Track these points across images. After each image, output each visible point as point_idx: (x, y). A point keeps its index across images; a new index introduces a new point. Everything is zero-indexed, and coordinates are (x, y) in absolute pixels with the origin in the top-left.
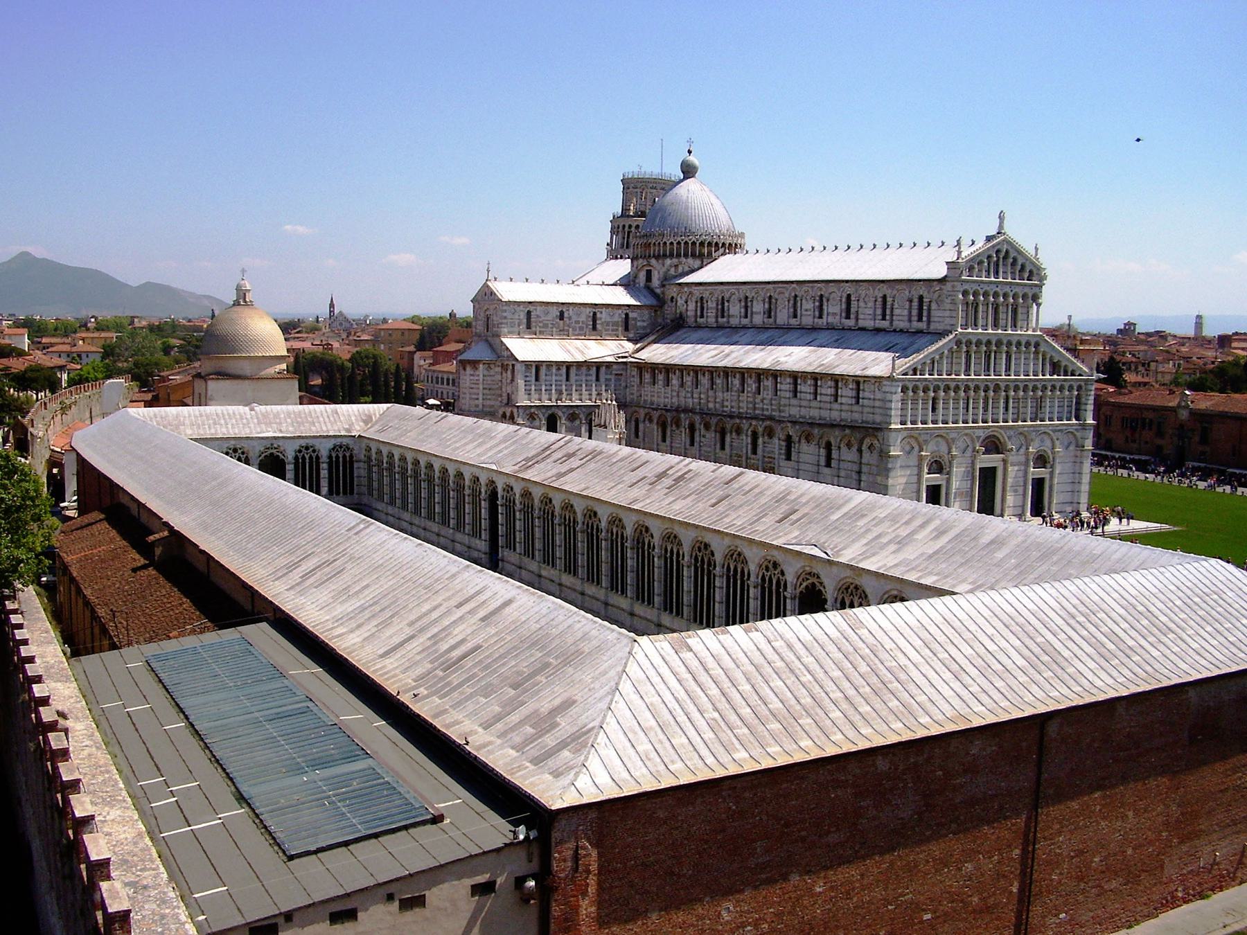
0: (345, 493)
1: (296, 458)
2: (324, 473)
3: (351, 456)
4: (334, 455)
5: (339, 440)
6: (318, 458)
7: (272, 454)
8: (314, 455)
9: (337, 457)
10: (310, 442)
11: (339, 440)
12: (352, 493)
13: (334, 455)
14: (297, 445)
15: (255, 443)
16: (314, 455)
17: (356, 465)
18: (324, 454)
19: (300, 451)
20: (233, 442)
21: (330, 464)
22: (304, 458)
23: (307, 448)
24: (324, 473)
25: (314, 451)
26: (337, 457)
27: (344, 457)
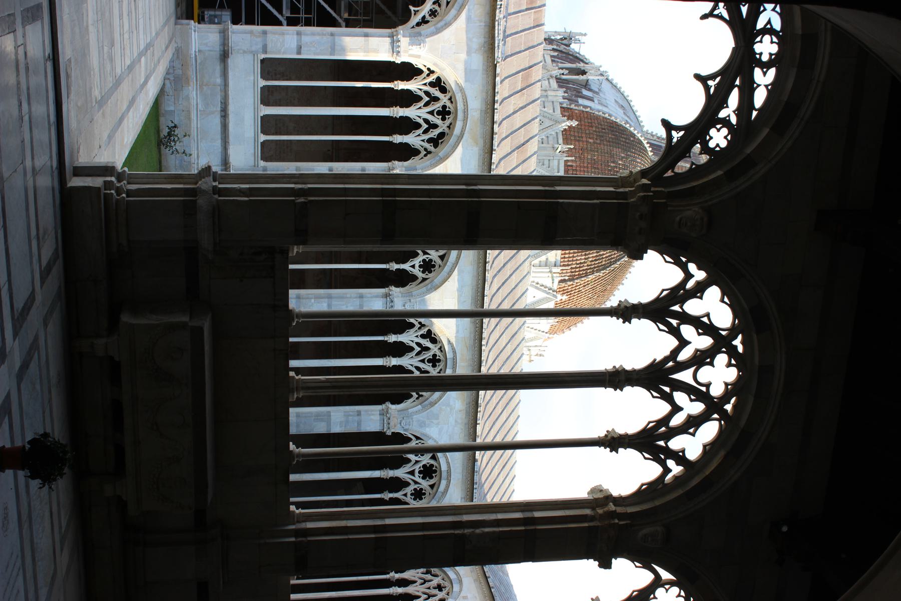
22: (398, 461)
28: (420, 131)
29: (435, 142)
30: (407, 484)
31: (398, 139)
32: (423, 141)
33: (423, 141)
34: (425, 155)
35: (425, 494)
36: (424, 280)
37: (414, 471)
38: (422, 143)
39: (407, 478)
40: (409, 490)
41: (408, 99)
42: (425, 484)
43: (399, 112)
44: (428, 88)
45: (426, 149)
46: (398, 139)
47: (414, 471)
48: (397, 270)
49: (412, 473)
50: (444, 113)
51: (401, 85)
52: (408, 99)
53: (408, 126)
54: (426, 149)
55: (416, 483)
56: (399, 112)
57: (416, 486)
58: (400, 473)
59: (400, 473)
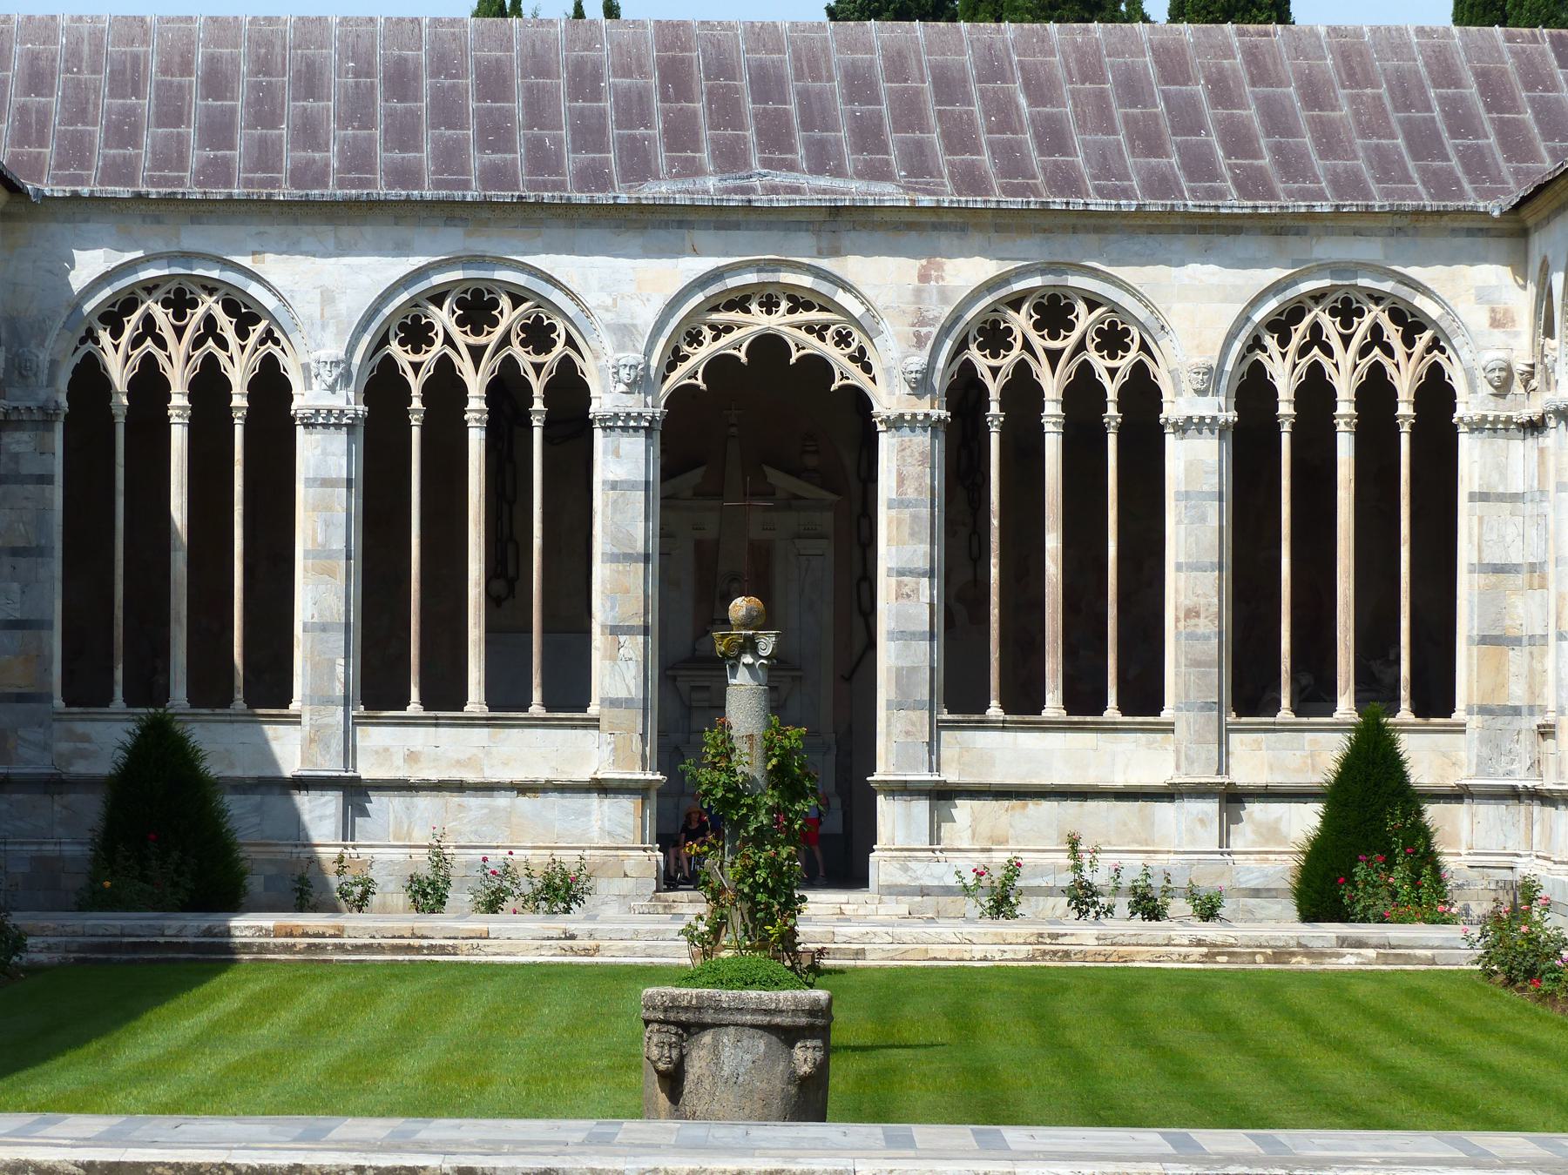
3: (1436, 393)
6: (1142, 393)
7: (769, 346)
13: (1284, 377)
21: (1250, 439)
22: (1023, 390)
28: (222, 356)
30: (1086, 369)
32: (243, 348)
33: (243, 348)
34: (277, 342)
35: (1113, 324)
36: (570, 342)
37: (1048, 351)
38: (248, 350)
39: (1066, 370)
40: (1100, 363)
42: (1084, 320)
44: (125, 339)
45: (262, 342)
47: (1048, 351)
48: (1121, 407)
49: (1054, 357)
54: (262, 342)
55: (1081, 346)
57: (515, 342)
58: (1052, 385)
59: (1052, 385)
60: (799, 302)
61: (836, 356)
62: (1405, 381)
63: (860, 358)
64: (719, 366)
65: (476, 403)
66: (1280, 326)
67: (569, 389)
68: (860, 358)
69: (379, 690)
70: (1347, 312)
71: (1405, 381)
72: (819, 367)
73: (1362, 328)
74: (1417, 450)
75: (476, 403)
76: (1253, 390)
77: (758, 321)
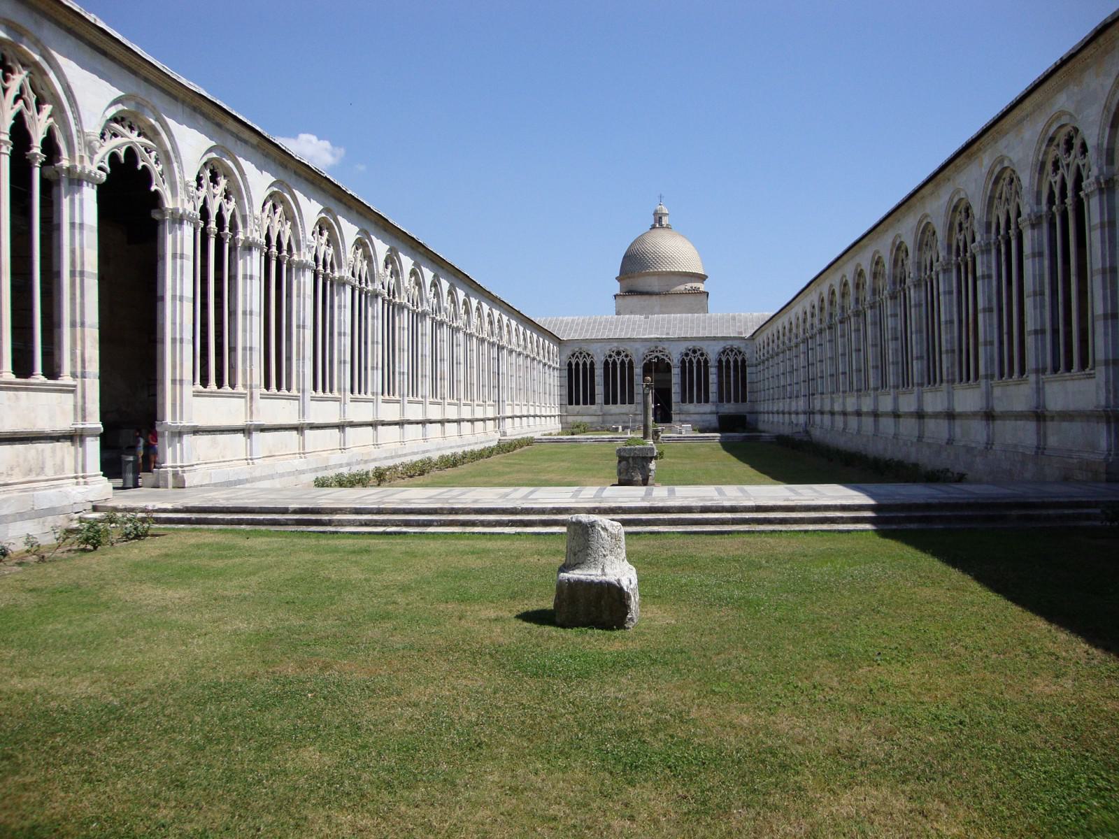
0: (736, 401)
1: (683, 362)
2: (713, 378)
3: (744, 361)
4: (724, 359)
5: (730, 343)
6: (706, 362)
8: (702, 359)
9: (728, 361)
10: (698, 345)
11: (730, 343)
12: (744, 400)
13: (724, 359)
14: (683, 347)
15: (637, 345)
16: (702, 359)
17: (748, 370)
18: (712, 358)
19: (687, 355)
20: (616, 344)
21: (720, 366)
22: (691, 362)
23: (694, 352)
24: (713, 378)
25: (702, 355)
26: (728, 361)
27: (736, 361)
29: (589, 355)
31: (588, 366)
41: (577, 364)
43: (581, 367)
46: (588, 366)
50: (581, 353)
51: (574, 367)
52: (577, 364)
53: (585, 364)
56: (581, 367)
58: (695, 361)
59: (695, 361)
60: (660, 351)
61: (666, 359)
62: (739, 359)
63: (669, 359)
64: (650, 360)
65: (618, 366)
66: (723, 352)
67: (631, 362)
68: (669, 359)
69: (607, 402)
70: (732, 351)
71: (739, 359)
72: (663, 359)
73: (734, 353)
74: (741, 367)
75: (618, 366)
76: (720, 361)
77: (656, 354)
